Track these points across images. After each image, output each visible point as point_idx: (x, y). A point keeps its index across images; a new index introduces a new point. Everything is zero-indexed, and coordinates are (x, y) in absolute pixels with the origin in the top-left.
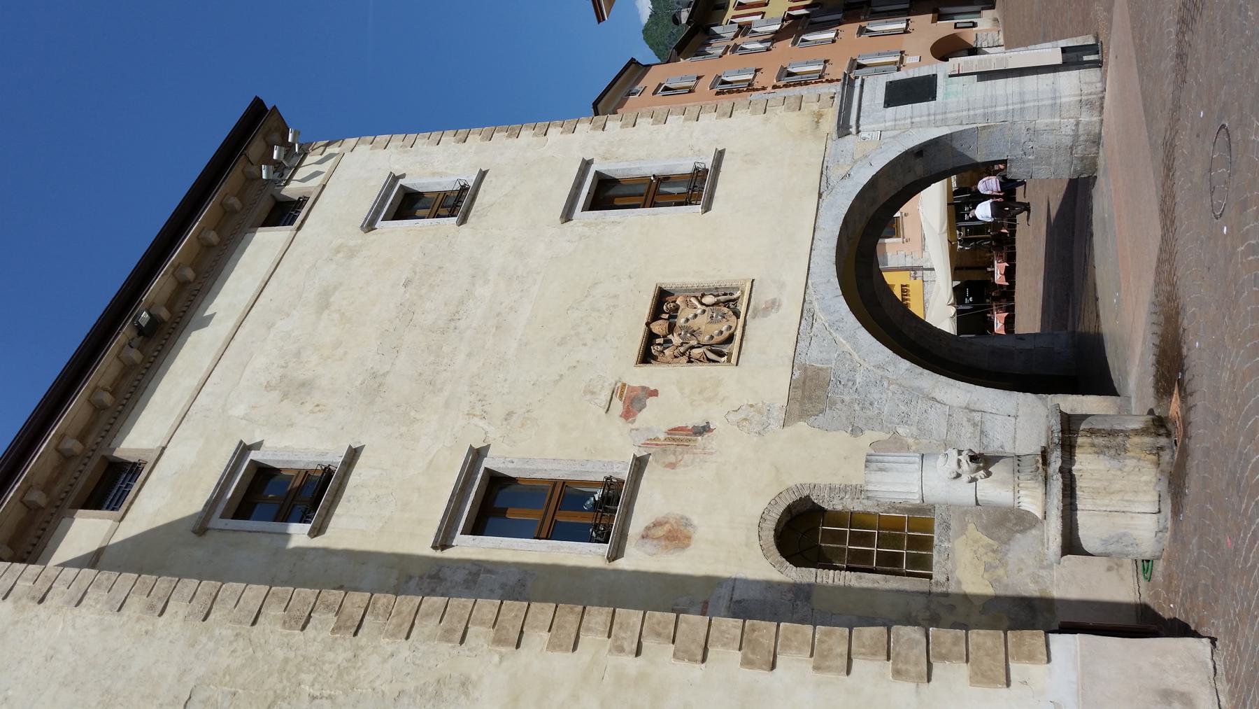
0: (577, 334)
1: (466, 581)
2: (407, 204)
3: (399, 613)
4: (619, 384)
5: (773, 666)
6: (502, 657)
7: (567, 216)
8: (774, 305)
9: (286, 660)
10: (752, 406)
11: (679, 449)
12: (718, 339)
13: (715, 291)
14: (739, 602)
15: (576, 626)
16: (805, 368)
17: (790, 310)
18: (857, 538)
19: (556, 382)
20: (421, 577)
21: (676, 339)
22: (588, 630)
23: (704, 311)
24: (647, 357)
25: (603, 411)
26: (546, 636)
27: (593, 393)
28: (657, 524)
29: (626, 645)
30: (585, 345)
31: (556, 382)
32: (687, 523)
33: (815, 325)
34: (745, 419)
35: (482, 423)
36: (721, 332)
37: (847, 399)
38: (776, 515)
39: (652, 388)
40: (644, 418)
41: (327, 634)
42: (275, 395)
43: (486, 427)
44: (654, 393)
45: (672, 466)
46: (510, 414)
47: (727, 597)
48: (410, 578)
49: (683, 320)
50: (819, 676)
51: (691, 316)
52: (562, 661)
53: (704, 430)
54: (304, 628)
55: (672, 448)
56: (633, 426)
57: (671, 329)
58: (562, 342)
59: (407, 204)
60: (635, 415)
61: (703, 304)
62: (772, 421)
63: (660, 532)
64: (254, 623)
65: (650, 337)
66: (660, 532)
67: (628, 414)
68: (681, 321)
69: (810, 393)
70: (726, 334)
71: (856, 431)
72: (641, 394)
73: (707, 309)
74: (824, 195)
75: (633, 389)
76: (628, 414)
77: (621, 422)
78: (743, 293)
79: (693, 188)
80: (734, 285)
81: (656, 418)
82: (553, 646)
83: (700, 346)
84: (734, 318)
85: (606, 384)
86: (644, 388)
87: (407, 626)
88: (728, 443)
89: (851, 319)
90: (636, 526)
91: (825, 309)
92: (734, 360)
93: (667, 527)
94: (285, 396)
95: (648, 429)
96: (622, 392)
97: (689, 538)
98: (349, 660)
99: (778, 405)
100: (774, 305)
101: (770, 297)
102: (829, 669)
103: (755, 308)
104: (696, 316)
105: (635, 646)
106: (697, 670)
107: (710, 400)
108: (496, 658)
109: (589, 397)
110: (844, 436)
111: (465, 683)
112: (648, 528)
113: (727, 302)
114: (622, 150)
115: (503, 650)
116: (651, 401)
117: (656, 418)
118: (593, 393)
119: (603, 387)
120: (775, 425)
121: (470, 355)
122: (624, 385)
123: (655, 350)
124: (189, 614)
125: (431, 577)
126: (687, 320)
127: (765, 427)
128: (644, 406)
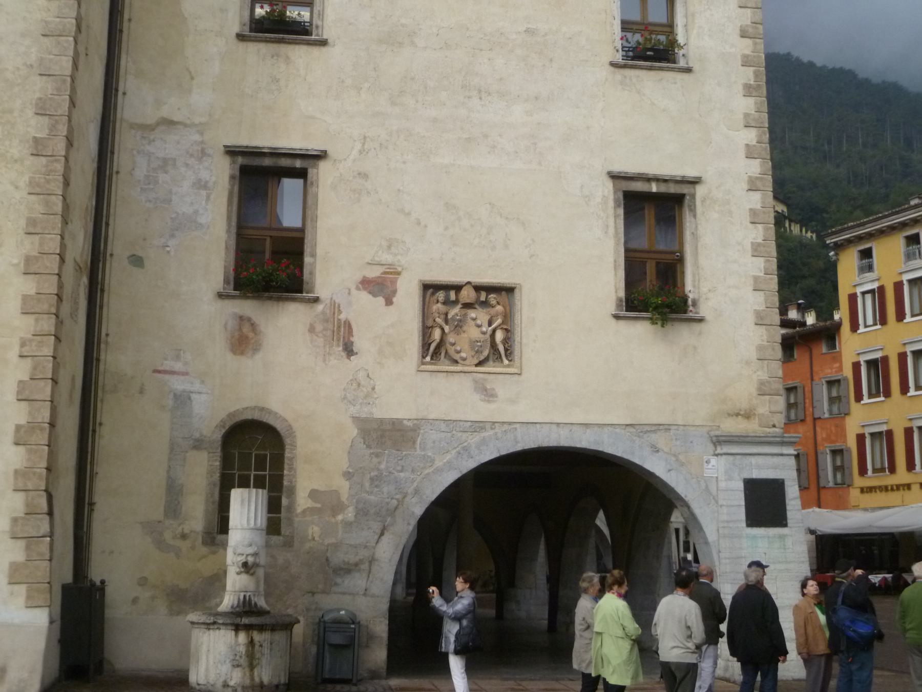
0: (459, 219)
1: (200, 180)
3: (48, 182)
4: (399, 269)
5: (17, 444)
6: (14, 265)
7: (615, 177)
8: (489, 395)
9: (11, 111)
10: (373, 389)
11: (329, 333)
12: (451, 350)
14: (190, 398)
15: (39, 311)
16: (416, 429)
17: (482, 411)
20: (202, 142)
21: (455, 311)
22: (37, 320)
23: (484, 333)
24: (430, 288)
25: (367, 260)
26: (32, 292)
27: (389, 247)
28: (253, 326)
29: (27, 348)
30: (446, 228)
32: (256, 350)
33: (465, 435)
34: (359, 385)
35: (355, 153)
36: (458, 352)
37: (383, 466)
39: (394, 300)
40: (364, 297)
41: (33, 133)
43: (352, 157)
44: (389, 302)
45: (312, 329)
47: (192, 389)
48: (202, 134)
50: (12, 474)
51: (479, 322)
52: (14, 305)
53: (349, 350)
54: (37, 114)
55: (330, 326)
56: (354, 291)
57: (468, 306)
60: (365, 289)
61: (494, 331)
62: (358, 407)
63: (246, 329)
64: (41, 75)
65: (458, 288)
66: (246, 329)
68: (472, 314)
69: (387, 436)
70: (457, 357)
71: (348, 475)
73: (488, 336)
74: (632, 430)
75: (394, 282)
77: (358, 277)
78: (508, 366)
80: (516, 358)
82: (25, 298)
84: (476, 361)
85: (399, 257)
86: (394, 292)
87: (38, 190)
88: (335, 373)
89: (471, 464)
90: (248, 307)
91: (484, 442)
92: (423, 367)
93: (251, 335)
96: (391, 273)
97: (242, 353)
98: (12, 157)
99: (374, 410)
100: (489, 395)
101: (500, 392)
102: (16, 478)
103: (485, 380)
104: (479, 326)
105: (25, 354)
108: (15, 261)
109: (385, 244)
110: (344, 465)
112: (249, 319)
113: (500, 350)
114: (716, 216)
115: (22, 265)
116: (381, 300)
117: (363, 309)
118: (389, 247)
119: (396, 255)
120: (353, 410)
121: (435, 120)
122: (399, 273)
123: (441, 295)
124: (46, 22)
125: (203, 150)
126: (474, 319)
127: (352, 403)
128: (375, 295)
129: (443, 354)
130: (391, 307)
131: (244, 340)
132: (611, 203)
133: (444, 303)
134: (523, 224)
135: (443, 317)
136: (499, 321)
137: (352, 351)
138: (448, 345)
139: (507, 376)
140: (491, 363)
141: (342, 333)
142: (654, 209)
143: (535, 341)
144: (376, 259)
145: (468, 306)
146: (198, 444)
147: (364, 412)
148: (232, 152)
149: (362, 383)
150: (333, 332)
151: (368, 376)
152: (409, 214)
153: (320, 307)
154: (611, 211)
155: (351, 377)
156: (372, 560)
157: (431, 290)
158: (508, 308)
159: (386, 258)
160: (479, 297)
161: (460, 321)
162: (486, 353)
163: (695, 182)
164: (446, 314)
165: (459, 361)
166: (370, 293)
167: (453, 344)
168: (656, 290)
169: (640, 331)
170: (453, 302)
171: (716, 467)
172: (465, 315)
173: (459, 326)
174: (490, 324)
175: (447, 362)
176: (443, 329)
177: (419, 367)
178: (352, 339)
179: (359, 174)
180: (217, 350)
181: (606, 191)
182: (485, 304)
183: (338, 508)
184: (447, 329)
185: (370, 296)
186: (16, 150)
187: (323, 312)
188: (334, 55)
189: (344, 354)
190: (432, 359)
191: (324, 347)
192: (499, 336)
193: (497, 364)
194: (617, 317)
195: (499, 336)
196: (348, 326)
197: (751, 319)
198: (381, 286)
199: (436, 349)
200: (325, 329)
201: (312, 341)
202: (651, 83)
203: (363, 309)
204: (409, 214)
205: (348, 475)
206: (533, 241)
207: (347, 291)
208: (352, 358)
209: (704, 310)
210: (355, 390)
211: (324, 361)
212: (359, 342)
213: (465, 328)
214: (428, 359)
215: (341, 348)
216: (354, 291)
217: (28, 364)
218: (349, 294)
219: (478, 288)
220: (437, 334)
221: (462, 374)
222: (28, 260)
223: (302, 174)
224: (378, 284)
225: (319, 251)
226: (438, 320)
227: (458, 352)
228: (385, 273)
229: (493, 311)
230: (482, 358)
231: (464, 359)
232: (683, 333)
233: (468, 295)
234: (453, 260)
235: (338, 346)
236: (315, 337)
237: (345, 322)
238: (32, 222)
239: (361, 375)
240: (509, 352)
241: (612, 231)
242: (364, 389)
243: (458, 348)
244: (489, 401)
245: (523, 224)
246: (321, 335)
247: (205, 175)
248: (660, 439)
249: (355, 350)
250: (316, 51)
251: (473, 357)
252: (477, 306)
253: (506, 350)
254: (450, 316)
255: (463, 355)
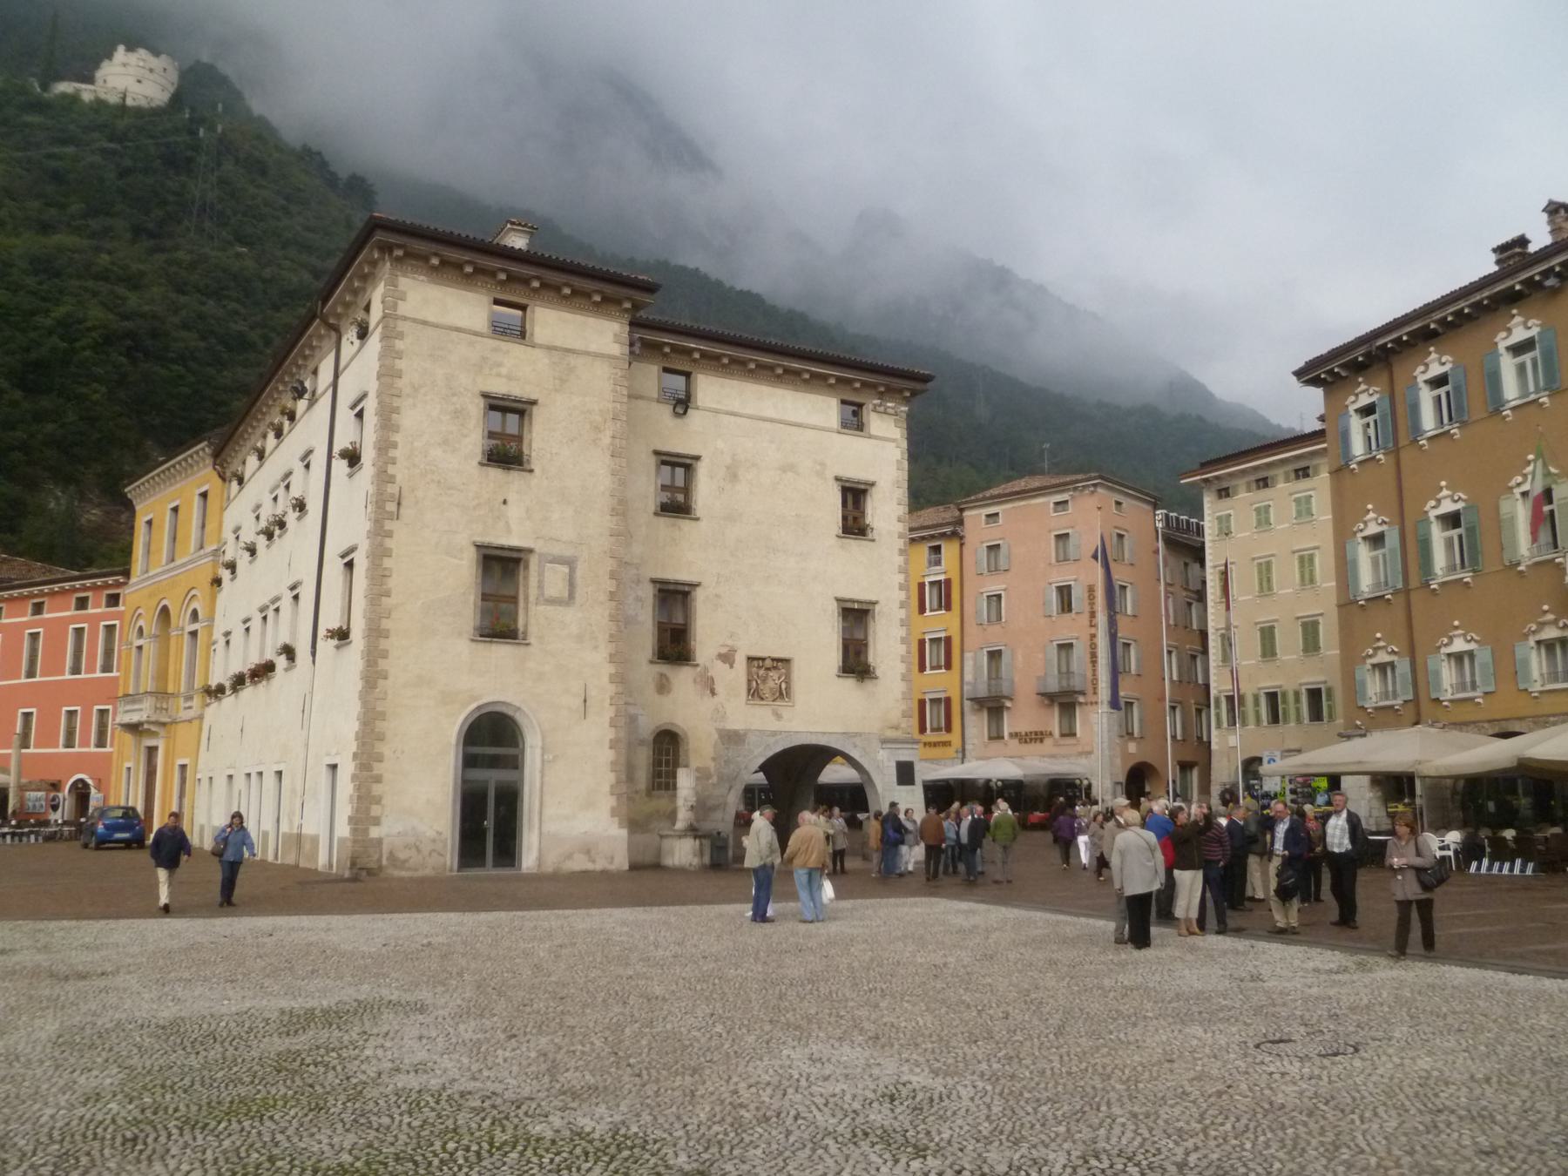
2: (854, 495)
7: (838, 600)
8: (778, 717)
17: (774, 725)
18: (667, 762)
21: (762, 672)
24: (750, 659)
28: (667, 679)
38: (674, 729)
40: (719, 663)
42: (729, 461)
52: (606, 679)
53: (713, 693)
57: (768, 669)
59: (854, 495)
65: (763, 659)
69: (732, 738)
71: (714, 759)
79: (856, 663)
81: (719, 670)
88: (708, 703)
89: (770, 754)
90: (664, 668)
94: (728, 468)
100: (778, 717)
106: (607, 725)
111: (596, 647)
113: (783, 694)
131: (663, 686)
142: (856, 616)
145: (768, 669)
146: (642, 742)
148: (654, 581)
156: (726, 804)
159: (730, 642)
163: (875, 603)
168: (856, 663)
169: (850, 683)
171: (883, 755)
180: (650, 689)
181: (833, 608)
183: (709, 776)
186: (603, 597)
188: (702, 524)
197: (899, 677)
198: (727, 658)
202: (854, 544)
205: (714, 759)
209: (878, 673)
212: (718, 688)
217: (613, 708)
222: (611, 655)
223: (686, 594)
232: (869, 684)
233: (768, 663)
238: (611, 636)
247: (640, 593)
248: (857, 740)
250: (693, 523)
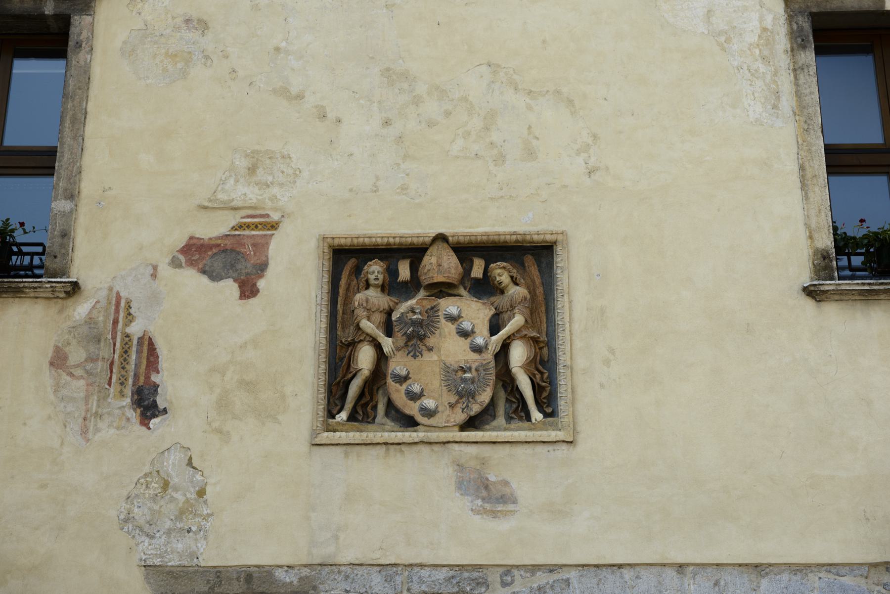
0: (417, 101)
4: (275, 216)
8: (492, 497)
10: (201, 493)
11: (101, 367)
13: (544, 365)
19: (283, 92)
21: (410, 306)
23: (478, 350)
27: (252, 170)
31: (283, 92)
34: (166, 485)
39: (261, 284)
40: (191, 281)
44: (248, 290)
45: (59, 360)
46: (203, 25)
49: (453, 310)
51: (466, 325)
53: (147, 406)
56: (165, 271)
58: (392, 76)
60: (191, 263)
62: (161, 540)
65: (415, 252)
67: (199, 254)
68: (450, 306)
70: (412, 409)
72: (245, 267)
73: (489, 356)
75: (261, 246)
76: (199, 254)
78: (542, 426)
80: (562, 405)
83: (381, 358)
85: (275, 190)
86: (262, 268)
95: (154, 299)
99: (202, 546)
100: (492, 497)
103: (484, 462)
107: (223, 405)
109: (242, 163)
113: (523, 392)
116: (230, 287)
118: (252, 170)
120: (147, 550)
122: (274, 226)
123: (375, 269)
126: (452, 319)
127: (147, 531)
128: (214, 277)
129: (381, 408)
130: (252, 301)
132: (782, 42)
133: (383, 288)
134: (570, 102)
135: (378, 317)
136: (517, 321)
137: (154, 405)
138: (389, 380)
139: (540, 449)
140: (501, 420)
141: (132, 367)
143: (607, 363)
144: (221, 196)
145: (442, 290)
147: (176, 552)
149: (175, 480)
150: (112, 364)
151: (190, 463)
152: (300, 97)
153: (81, 309)
154: (783, 61)
155: (147, 469)
157: (352, 262)
158: (540, 290)
159: (245, 193)
160: (467, 271)
161: (419, 324)
162: (485, 397)
164: (389, 313)
165: (419, 418)
166: (204, 272)
167: (402, 379)
170: (405, 283)
172: (434, 309)
173: (417, 337)
174: (494, 329)
175: (390, 424)
176: (378, 347)
177: (314, 434)
178: (155, 378)
179: (188, 21)
182: (484, 288)
184: (387, 344)
185: (204, 279)
187: (90, 321)
189: (133, 415)
190: (352, 418)
191: (87, 399)
192: (518, 354)
193: (516, 423)
194: (812, 293)
195: (518, 354)
196: (150, 351)
198: (232, 258)
199: (361, 395)
200: (92, 359)
201: (57, 389)
203: (191, 316)
204: (300, 97)
206: (595, 137)
207: (150, 270)
208: (154, 422)
210: (155, 498)
211: (84, 432)
212: (172, 385)
213: (431, 341)
214: (343, 416)
215: (128, 401)
216: (165, 271)
218: (154, 276)
219: (466, 251)
220: (365, 358)
221: (425, 449)
224: (225, 251)
225: (88, 186)
226: (367, 325)
227: (414, 397)
228: (241, 227)
229: (502, 301)
230: (476, 409)
231: (429, 413)
234: (404, 188)
235: (122, 394)
236: (66, 378)
237: (141, 340)
239: (173, 464)
240: (547, 399)
241: (787, 102)
242: (179, 496)
243: (416, 388)
244: (494, 514)
245: (570, 102)
246: (79, 372)
249: (161, 404)
251: (452, 406)
252: (462, 291)
253: (537, 389)
254: (395, 316)
255: (430, 403)
